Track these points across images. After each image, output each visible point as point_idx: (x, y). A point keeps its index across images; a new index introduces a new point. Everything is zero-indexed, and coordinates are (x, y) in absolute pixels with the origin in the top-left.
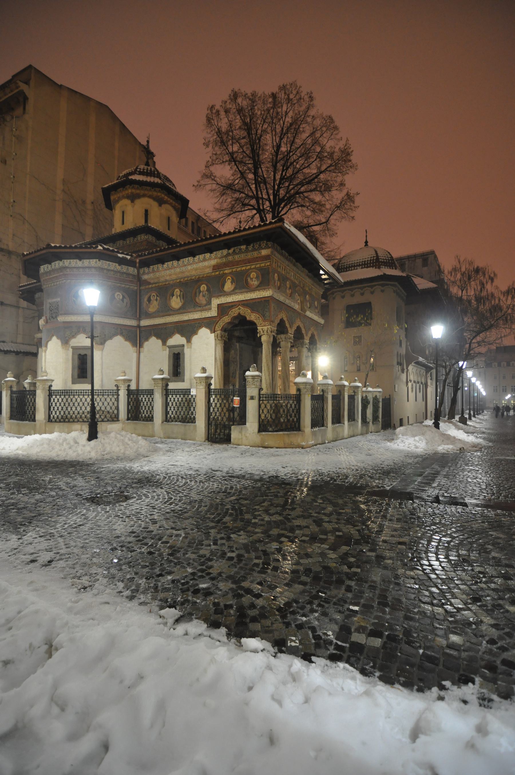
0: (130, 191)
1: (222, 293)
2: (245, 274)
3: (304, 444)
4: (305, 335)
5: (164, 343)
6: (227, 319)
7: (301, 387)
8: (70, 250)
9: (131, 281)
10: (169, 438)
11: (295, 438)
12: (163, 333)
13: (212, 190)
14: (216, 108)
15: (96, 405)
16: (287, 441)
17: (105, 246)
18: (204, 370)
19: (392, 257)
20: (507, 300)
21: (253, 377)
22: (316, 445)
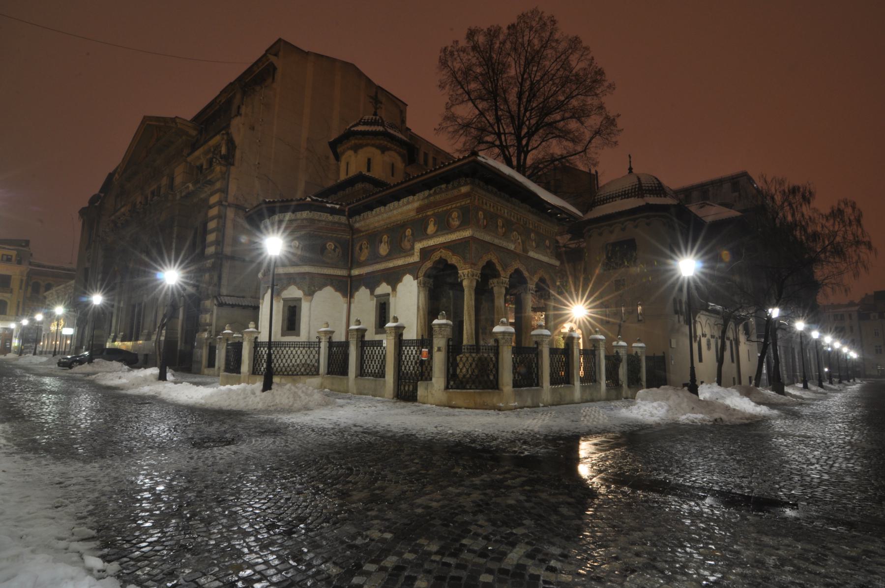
1: (426, 236)
2: (448, 213)
3: (501, 405)
4: (528, 279)
5: (372, 293)
6: (429, 264)
7: (500, 337)
10: (361, 394)
11: (492, 398)
12: (371, 282)
13: (456, 131)
14: (449, 49)
15: (273, 357)
19: (660, 183)
20: (834, 225)
21: (440, 325)
22: (521, 408)
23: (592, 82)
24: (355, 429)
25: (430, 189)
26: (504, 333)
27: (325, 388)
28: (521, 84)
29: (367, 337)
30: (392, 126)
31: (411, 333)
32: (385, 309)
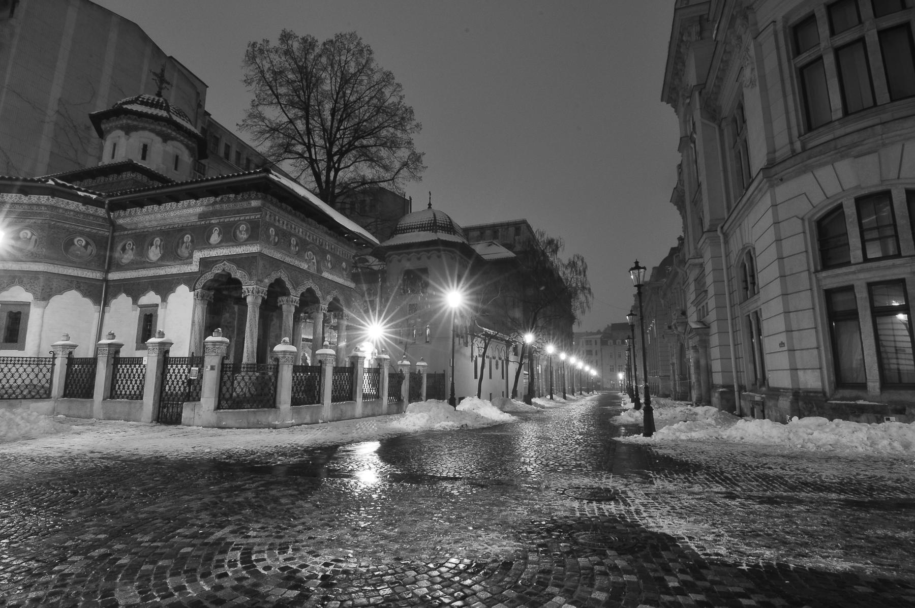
0: (125, 121)
3: (277, 423)
5: (135, 301)
6: (209, 276)
7: (280, 356)
8: (9, 183)
9: (100, 225)
10: (109, 419)
12: (134, 289)
13: (262, 133)
14: (258, 46)
16: (252, 419)
17: (59, 181)
18: (162, 335)
19: (451, 222)
21: (214, 343)
23: (401, 117)
24: (92, 455)
25: (216, 196)
26: (285, 352)
27: (58, 414)
28: (336, 102)
29: (123, 354)
30: (180, 113)
31: (181, 349)
32: (151, 321)
